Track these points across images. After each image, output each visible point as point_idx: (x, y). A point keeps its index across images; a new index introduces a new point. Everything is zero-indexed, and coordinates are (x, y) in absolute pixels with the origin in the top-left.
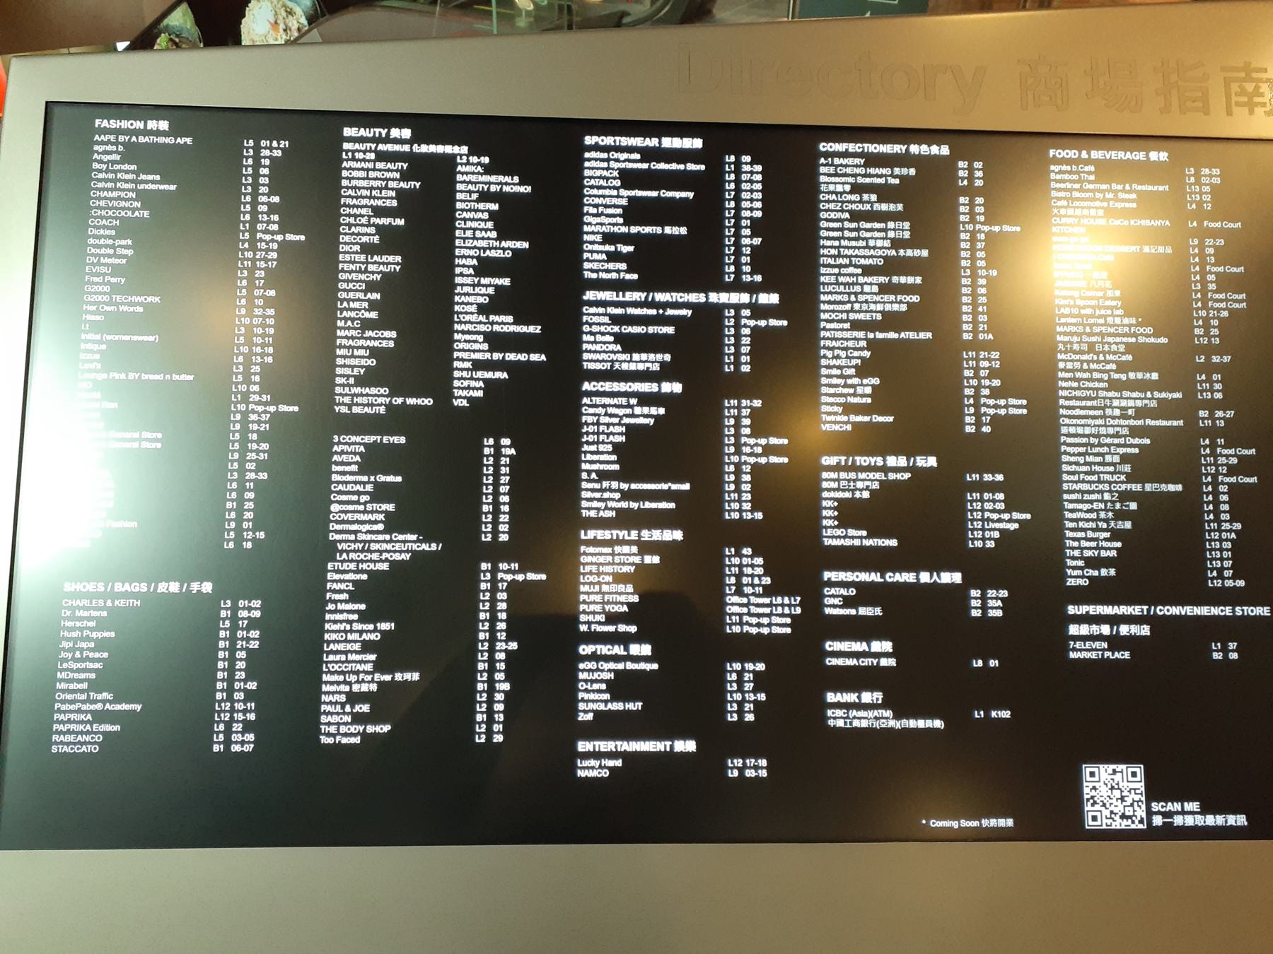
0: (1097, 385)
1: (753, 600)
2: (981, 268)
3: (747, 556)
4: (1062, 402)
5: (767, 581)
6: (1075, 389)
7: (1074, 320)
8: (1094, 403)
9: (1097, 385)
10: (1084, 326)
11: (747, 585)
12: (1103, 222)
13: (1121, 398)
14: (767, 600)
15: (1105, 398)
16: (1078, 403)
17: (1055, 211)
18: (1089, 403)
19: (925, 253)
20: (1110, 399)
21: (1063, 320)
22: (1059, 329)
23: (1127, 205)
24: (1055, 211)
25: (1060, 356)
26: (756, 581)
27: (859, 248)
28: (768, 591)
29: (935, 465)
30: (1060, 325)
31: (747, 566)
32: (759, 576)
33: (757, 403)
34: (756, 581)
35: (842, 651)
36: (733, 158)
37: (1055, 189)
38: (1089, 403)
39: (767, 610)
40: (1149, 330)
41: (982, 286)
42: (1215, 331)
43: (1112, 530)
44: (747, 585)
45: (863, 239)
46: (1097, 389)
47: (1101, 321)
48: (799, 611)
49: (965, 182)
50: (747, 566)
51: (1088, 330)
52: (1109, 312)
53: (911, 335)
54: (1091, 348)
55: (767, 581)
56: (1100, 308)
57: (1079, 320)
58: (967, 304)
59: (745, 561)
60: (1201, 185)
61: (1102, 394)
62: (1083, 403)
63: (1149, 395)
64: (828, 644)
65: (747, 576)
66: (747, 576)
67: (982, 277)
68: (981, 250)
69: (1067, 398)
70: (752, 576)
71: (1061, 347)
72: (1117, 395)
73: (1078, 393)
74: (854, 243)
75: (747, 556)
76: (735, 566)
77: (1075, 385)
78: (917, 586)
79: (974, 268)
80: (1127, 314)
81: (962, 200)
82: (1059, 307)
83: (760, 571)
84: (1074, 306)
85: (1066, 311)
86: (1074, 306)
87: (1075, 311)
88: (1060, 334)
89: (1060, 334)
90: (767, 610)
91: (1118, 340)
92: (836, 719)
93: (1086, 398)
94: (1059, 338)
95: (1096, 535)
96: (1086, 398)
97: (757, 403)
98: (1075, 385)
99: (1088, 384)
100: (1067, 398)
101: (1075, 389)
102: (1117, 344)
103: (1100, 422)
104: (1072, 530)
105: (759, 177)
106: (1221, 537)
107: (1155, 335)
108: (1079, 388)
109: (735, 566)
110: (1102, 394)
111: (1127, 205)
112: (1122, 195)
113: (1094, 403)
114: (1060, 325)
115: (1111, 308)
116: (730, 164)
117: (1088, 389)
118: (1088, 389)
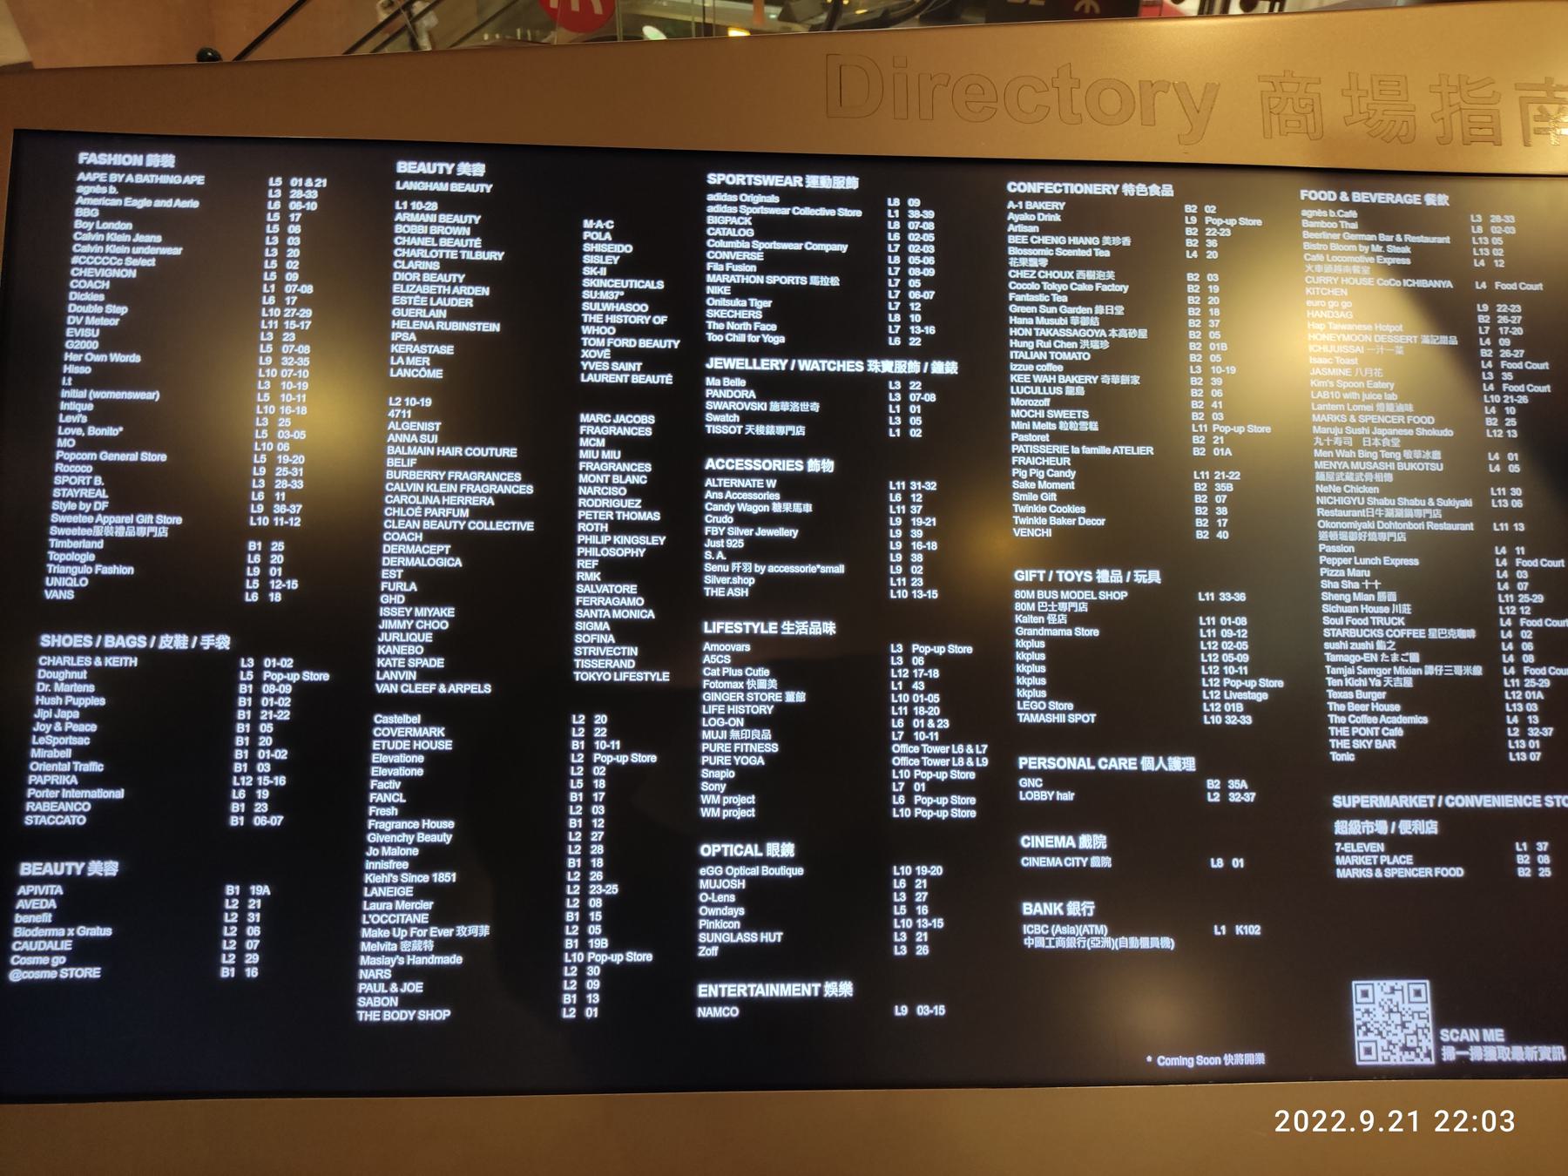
0: (1365, 489)
1: (927, 748)
2: (1216, 364)
3: (919, 692)
4: (1320, 511)
5: (945, 724)
6: (1337, 495)
7: (1335, 407)
8: (1362, 513)
9: (1365, 489)
10: (1348, 414)
11: (919, 729)
12: (1369, 282)
13: (1397, 506)
14: (944, 749)
15: (1375, 507)
16: (1341, 513)
17: (1309, 267)
18: (1356, 513)
19: (1143, 334)
20: (1383, 507)
21: (1321, 407)
22: (1315, 418)
23: (1399, 261)
24: (1309, 267)
25: (1317, 453)
26: (931, 724)
27: (1058, 327)
28: (946, 737)
29: (1158, 580)
30: (1317, 412)
31: (919, 704)
32: (935, 718)
33: (931, 486)
34: (931, 724)
35: (1042, 848)
36: (897, 202)
37: (1309, 240)
38: (1356, 513)
39: (944, 762)
40: (1430, 420)
41: (1217, 387)
42: (1512, 422)
43: (1388, 689)
44: (919, 729)
45: (1064, 316)
46: (1366, 495)
47: (1369, 408)
48: (985, 762)
49: (1195, 255)
50: (919, 704)
51: (1353, 419)
52: (1379, 396)
53: (1127, 450)
54: (1358, 443)
55: (945, 724)
56: (1367, 391)
57: (1341, 407)
58: (1198, 410)
59: (916, 698)
60: (1490, 236)
61: (1372, 501)
62: (1348, 513)
63: (1431, 502)
64: (1023, 839)
65: (919, 717)
66: (919, 717)
67: (1216, 376)
68: (1214, 329)
69: (1327, 507)
70: (926, 718)
71: (1318, 441)
72: (1392, 502)
73: (1342, 501)
74: (1052, 321)
75: (919, 692)
76: (903, 704)
77: (1337, 489)
78: (1139, 774)
79: (1206, 364)
80: (1402, 399)
81: (1190, 277)
82: (1316, 390)
83: (935, 711)
84: (1335, 389)
85: (1325, 395)
86: (1335, 389)
87: (1336, 395)
88: (1317, 424)
89: (1317, 424)
90: (944, 762)
91: (1391, 432)
92: (1035, 938)
93: (1351, 507)
94: (1316, 430)
95: (1368, 695)
96: (1351, 507)
97: (931, 486)
98: (1337, 489)
99: (1353, 489)
100: (1327, 507)
101: (1337, 495)
102: (1390, 437)
103: (1369, 525)
104: (1337, 689)
105: (931, 226)
106: (1528, 687)
107: (1438, 426)
108: (1343, 494)
109: (903, 704)
110: (1372, 501)
111: (1399, 261)
112: (1391, 249)
113: (1362, 513)
114: (1317, 412)
115: (1381, 391)
116: (893, 208)
117: (1354, 495)
118: (1354, 495)
